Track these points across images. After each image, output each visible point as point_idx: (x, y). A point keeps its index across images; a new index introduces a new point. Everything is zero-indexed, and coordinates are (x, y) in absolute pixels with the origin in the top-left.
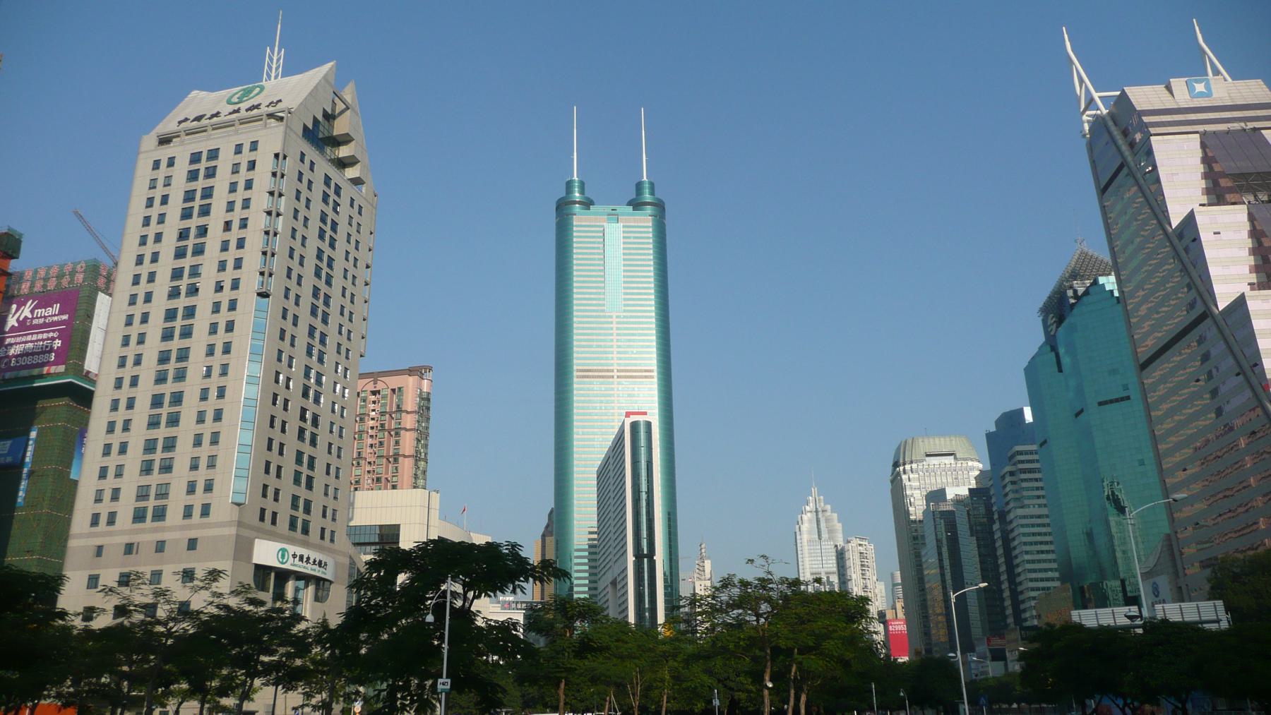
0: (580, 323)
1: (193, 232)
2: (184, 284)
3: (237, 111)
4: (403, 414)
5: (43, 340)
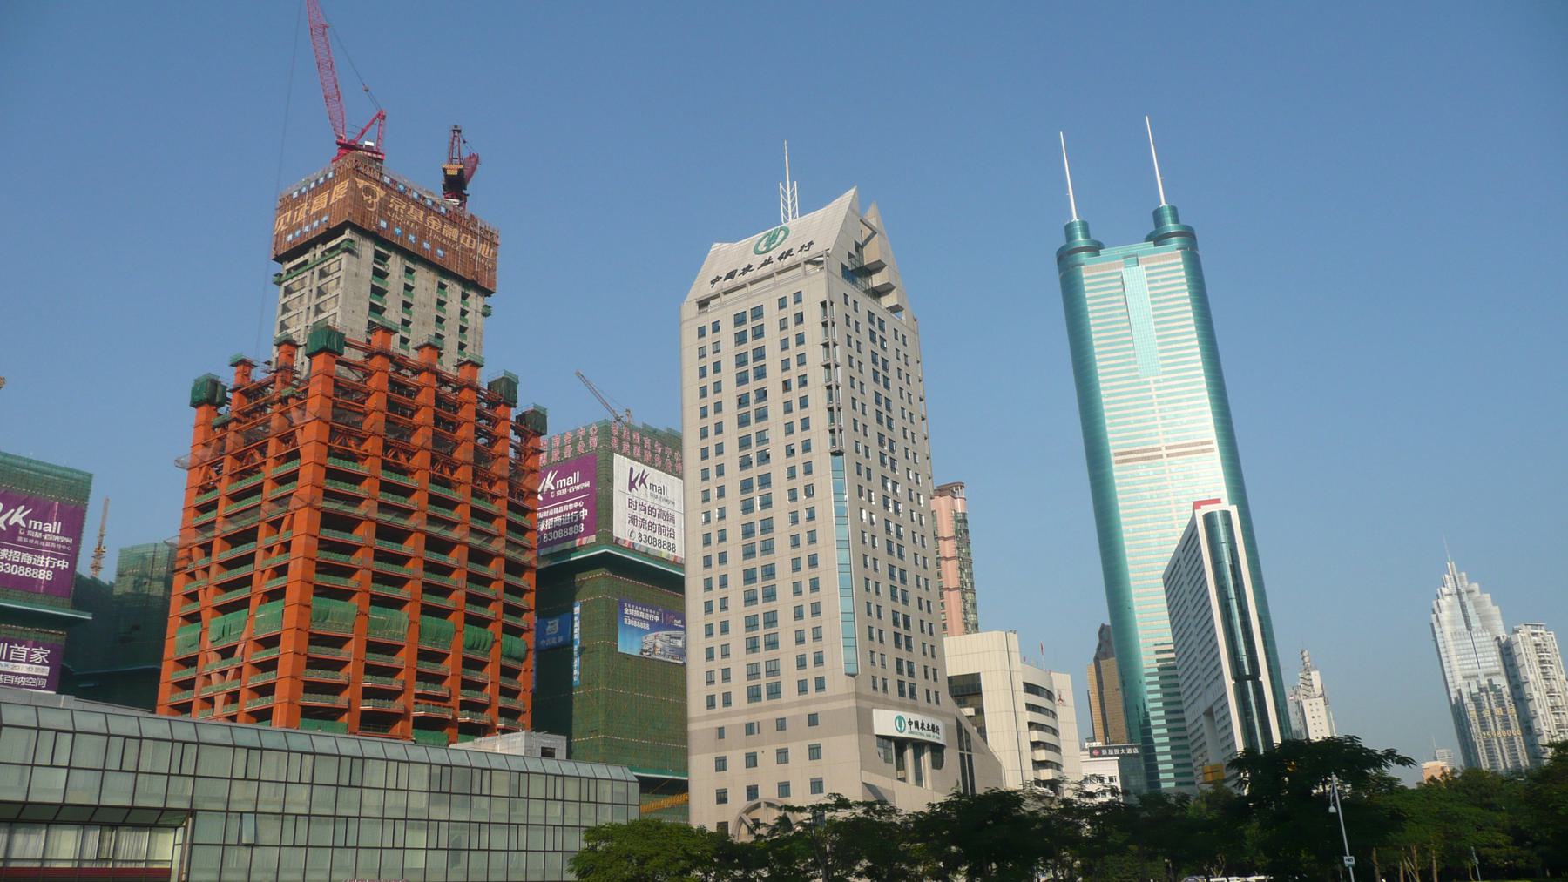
0: (1109, 395)
1: (752, 397)
2: (753, 452)
3: (769, 261)
4: (941, 541)
5: (570, 511)
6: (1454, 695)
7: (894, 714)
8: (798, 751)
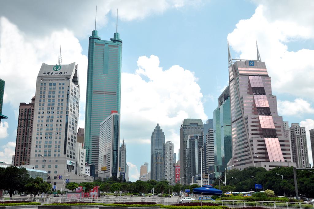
8: (53, 166)
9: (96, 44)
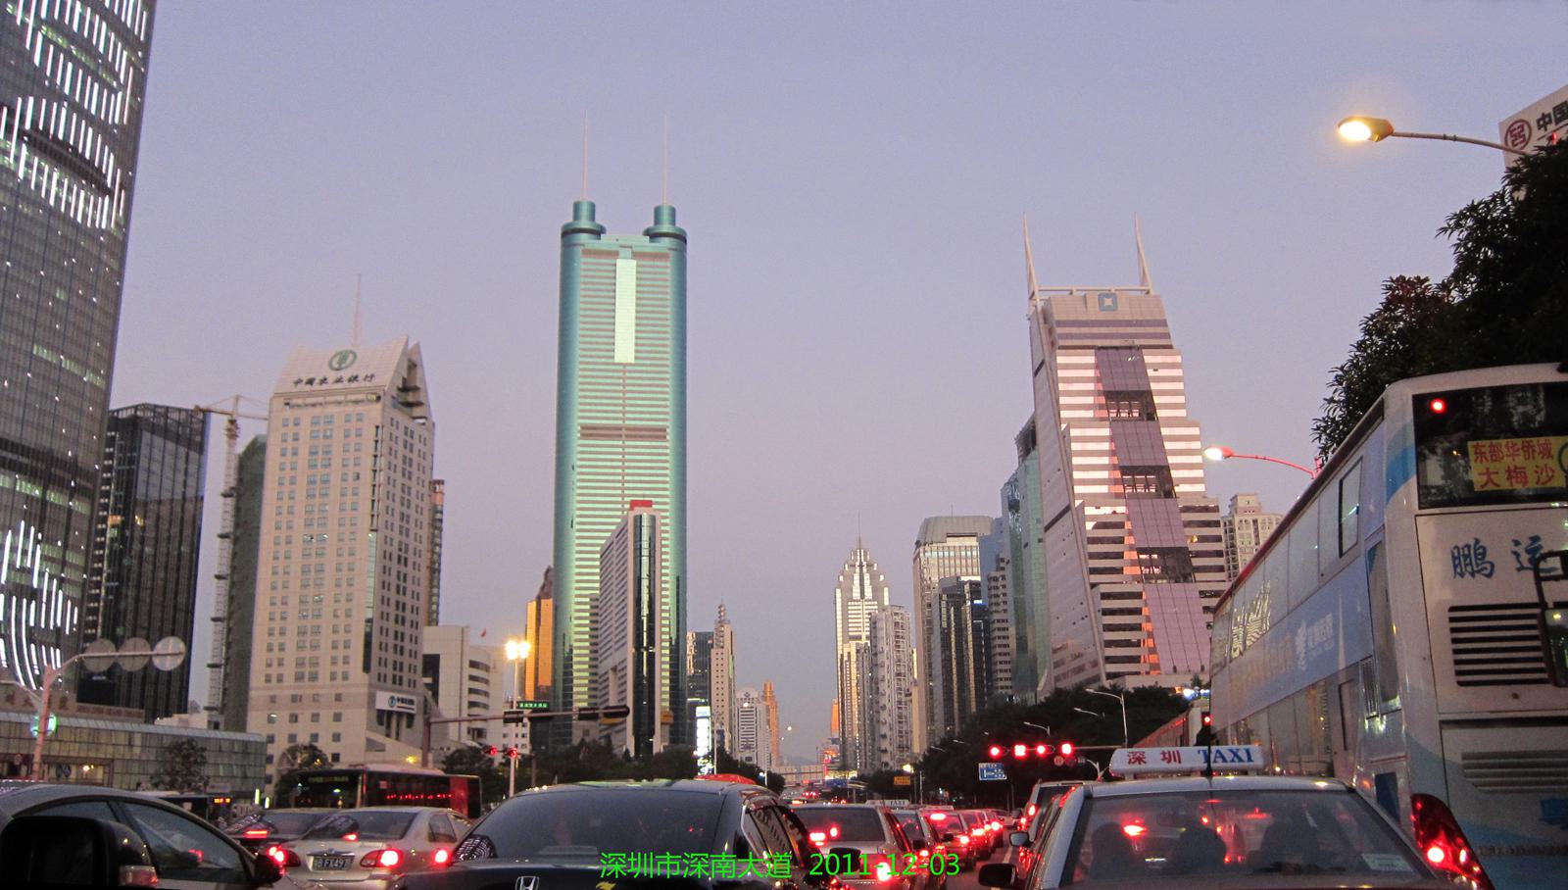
6: (840, 652)
7: (389, 695)
8: (326, 715)
9: (588, 253)
